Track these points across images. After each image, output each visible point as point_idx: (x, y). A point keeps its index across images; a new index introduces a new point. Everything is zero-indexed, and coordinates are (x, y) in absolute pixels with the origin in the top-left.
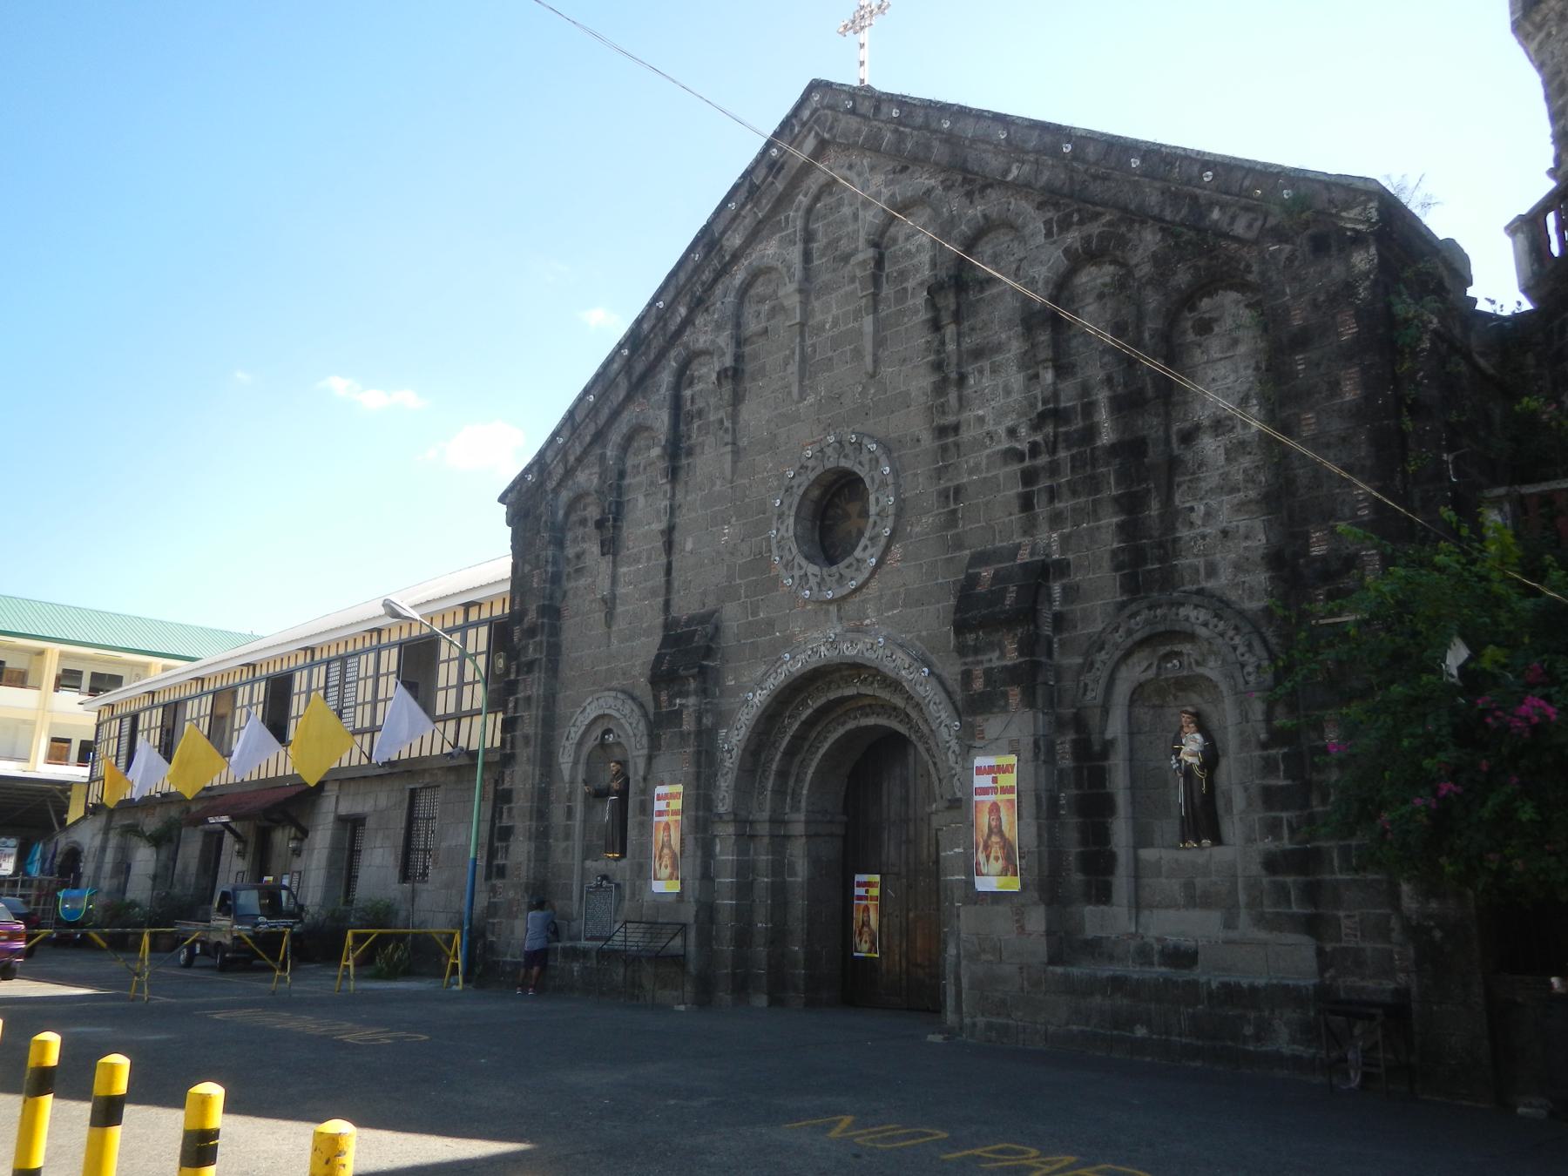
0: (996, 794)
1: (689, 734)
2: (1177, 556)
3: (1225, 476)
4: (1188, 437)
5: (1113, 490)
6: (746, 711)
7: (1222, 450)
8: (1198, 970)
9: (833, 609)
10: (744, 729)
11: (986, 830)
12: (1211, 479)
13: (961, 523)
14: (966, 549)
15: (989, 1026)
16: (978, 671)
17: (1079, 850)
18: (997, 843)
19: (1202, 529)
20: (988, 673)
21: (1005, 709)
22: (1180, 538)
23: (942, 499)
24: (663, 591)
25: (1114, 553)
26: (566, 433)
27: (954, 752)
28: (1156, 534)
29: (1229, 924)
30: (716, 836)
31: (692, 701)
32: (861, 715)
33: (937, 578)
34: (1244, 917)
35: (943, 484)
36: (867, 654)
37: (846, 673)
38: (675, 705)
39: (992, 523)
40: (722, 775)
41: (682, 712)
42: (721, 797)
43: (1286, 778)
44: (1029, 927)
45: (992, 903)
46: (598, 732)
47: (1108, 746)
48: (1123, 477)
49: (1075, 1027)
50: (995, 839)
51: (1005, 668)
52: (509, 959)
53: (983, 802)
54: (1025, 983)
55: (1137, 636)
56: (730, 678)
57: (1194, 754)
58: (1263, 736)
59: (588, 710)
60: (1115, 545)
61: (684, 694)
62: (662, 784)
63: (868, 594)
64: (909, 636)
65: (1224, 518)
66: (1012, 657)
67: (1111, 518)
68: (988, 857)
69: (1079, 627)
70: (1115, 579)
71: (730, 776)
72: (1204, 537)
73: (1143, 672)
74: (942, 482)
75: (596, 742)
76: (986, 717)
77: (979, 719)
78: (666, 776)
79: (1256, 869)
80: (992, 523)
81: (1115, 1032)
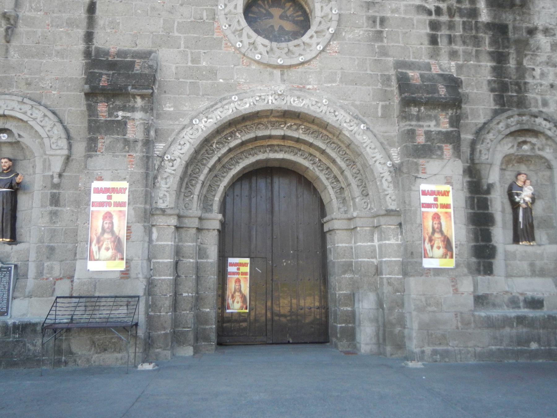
0: (437, 208)
1: (136, 141)
2: (526, 91)
3: (549, 57)
4: (532, 32)
5: (487, 47)
6: (191, 132)
7: (549, 44)
8: (545, 309)
9: (277, 72)
11: (430, 230)
12: (542, 57)
13: (385, 40)
14: (389, 56)
15: (435, 352)
16: (420, 132)
17: (473, 244)
18: (438, 238)
19: (539, 81)
20: (428, 134)
21: (441, 157)
22: (528, 83)
23: (371, 22)
24: (85, 23)
25: (489, 82)
27: (386, 180)
28: (514, 77)
30: (153, 226)
31: (139, 115)
33: (366, 70)
35: (371, 13)
36: (312, 108)
37: (274, 119)
39: (408, 46)
40: (162, 179)
41: (126, 124)
42: (161, 195)
44: (461, 289)
45: (434, 275)
47: (490, 187)
48: (493, 42)
49: (493, 347)
50: (437, 235)
51: (440, 132)
53: (427, 212)
54: (459, 323)
55: (513, 129)
56: (168, 105)
57: (527, 196)
60: (489, 78)
61: (133, 109)
62: (100, 179)
63: (309, 68)
64: (346, 102)
66: (445, 126)
67: (487, 62)
68: (432, 247)
69: (470, 117)
70: (490, 96)
72: (541, 85)
73: (509, 149)
74: (370, 11)
76: (427, 160)
77: (421, 161)
81: (519, 348)
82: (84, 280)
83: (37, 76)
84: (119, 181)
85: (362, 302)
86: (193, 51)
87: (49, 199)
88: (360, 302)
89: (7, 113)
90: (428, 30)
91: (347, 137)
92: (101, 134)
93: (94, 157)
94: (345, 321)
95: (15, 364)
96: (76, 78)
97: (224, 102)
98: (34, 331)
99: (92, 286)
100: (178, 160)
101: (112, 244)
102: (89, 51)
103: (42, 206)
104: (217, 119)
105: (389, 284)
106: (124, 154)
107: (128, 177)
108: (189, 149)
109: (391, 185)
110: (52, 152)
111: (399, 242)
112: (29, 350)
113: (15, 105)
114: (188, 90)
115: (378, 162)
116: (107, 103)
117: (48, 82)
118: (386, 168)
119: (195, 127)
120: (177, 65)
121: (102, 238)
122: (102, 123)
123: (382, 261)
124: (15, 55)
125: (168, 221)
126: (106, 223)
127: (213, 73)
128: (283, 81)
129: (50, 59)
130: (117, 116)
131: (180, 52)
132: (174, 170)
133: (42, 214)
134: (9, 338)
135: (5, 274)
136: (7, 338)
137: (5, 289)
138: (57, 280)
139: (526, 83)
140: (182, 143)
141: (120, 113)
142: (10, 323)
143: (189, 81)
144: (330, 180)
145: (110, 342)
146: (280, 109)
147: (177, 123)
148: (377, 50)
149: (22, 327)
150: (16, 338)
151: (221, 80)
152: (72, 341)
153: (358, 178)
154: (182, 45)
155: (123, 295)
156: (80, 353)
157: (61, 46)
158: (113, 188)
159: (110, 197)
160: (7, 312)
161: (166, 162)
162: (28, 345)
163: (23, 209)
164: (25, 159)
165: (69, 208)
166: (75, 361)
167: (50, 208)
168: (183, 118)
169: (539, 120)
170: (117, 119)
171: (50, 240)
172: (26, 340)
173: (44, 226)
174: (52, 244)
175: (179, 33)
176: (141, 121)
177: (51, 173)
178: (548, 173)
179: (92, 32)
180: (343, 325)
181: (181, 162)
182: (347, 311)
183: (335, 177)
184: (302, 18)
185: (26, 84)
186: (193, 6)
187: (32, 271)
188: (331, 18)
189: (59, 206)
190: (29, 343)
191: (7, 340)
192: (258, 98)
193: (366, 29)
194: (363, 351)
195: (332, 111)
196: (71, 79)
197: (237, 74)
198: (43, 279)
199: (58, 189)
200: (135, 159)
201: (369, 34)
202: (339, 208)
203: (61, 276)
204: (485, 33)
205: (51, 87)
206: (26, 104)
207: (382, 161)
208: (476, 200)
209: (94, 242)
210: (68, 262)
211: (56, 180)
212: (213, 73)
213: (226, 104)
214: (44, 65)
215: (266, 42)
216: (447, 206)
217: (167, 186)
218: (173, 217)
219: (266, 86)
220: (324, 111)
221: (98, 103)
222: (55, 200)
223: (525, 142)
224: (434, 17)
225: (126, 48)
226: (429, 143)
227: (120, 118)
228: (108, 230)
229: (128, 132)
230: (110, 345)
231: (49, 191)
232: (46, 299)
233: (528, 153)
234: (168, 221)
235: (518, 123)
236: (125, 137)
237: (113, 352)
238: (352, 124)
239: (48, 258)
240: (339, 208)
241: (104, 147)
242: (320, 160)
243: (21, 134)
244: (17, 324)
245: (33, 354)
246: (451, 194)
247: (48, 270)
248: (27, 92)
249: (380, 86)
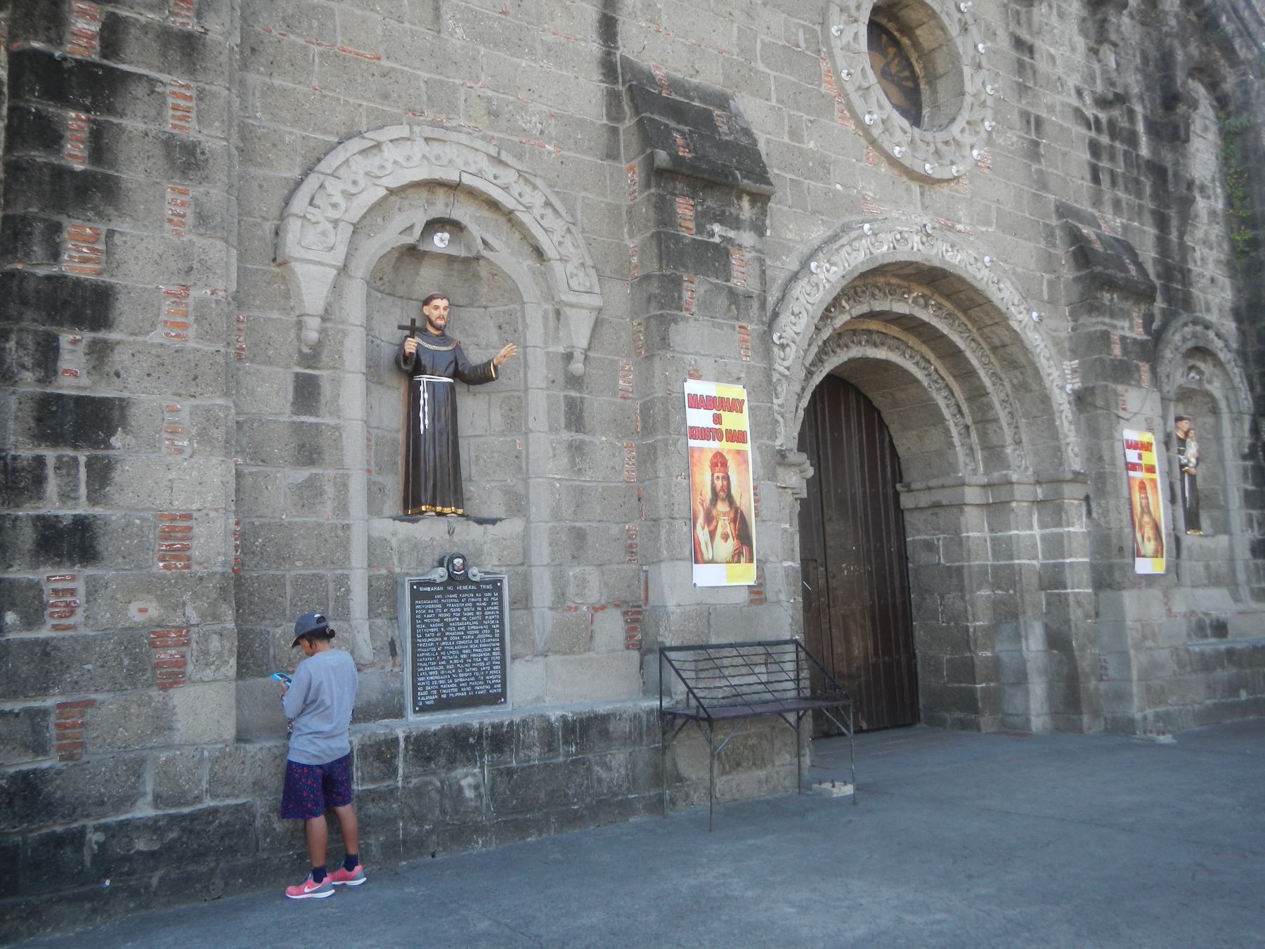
9: (915, 188)
10: (804, 319)
12: (1199, 234)
14: (1050, 192)
16: (1115, 336)
21: (1139, 386)
29: (1237, 599)
32: (867, 341)
34: (1244, 592)
37: (893, 281)
38: (713, 235)
39: (1068, 178)
41: (727, 254)
43: (1253, 485)
46: (419, 219)
48: (1155, 196)
52: (144, 810)
58: (1246, 450)
59: (390, 153)
62: (696, 375)
63: (957, 191)
74: (1024, 102)
75: (410, 240)
77: (1120, 388)
78: (706, 364)
79: (1248, 555)
80: (1068, 178)
82: (688, 608)
83: (511, 98)
84: (728, 382)
85: (1027, 639)
86: (792, 113)
87: (562, 412)
88: (1023, 641)
89: (467, 180)
90: (1087, 156)
91: (1015, 331)
92: (687, 271)
93: (681, 323)
94: (987, 679)
95: (573, 819)
96: (592, 123)
97: (853, 234)
98: (605, 734)
99: (704, 621)
101: (732, 524)
102: (611, 62)
103: (553, 430)
104: (844, 267)
105: (1079, 603)
106: (731, 322)
107: (743, 375)
108: (808, 325)
109: (1073, 427)
110: (572, 298)
111: (1084, 530)
112: (600, 781)
113: (484, 163)
114: (789, 197)
115: (1055, 384)
116: (693, 199)
117: (535, 119)
118: (1064, 396)
119: (814, 278)
120: (768, 136)
121: (714, 512)
122: (686, 244)
123: (1063, 564)
124: (457, 30)
125: (787, 477)
126: (718, 478)
127: (823, 167)
128: (925, 207)
129: (535, 61)
130: (713, 235)
131: (772, 108)
132: (788, 368)
133: (554, 449)
134: (558, 756)
135: (489, 597)
136: (553, 757)
137: (494, 637)
138: (596, 610)
139: (1189, 271)
140: (796, 310)
141: (717, 228)
142: (553, 719)
143: (789, 176)
144: (952, 409)
145: (745, 746)
146: (928, 264)
147: (778, 264)
148: (1035, 177)
149: (581, 728)
150: (572, 755)
151: (838, 187)
152: (678, 750)
153: (1007, 410)
154: (774, 96)
155: (758, 638)
156: (694, 777)
157: (554, 34)
158: (722, 399)
159: (717, 419)
160: (503, 694)
161: (776, 349)
162: (597, 768)
163: (470, 432)
164: (471, 305)
165: (604, 439)
166: (687, 795)
167: (567, 436)
168: (787, 256)
169: (1211, 334)
170: (712, 240)
171: (575, 513)
172: (590, 756)
173: (560, 479)
174: (578, 524)
175: (768, 65)
176: (754, 254)
177: (561, 350)
178: (1210, 420)
179: (612, 18)
180: (984, 685)
181: (797, 351)
182: (987, 658)
183: (958, 406)
184: (910, 84)
185: (489, 113)
186: (783, 12)
187: (543, 594)
188: (984, 101)
189: (584, 433)
190: (597, 764)
191: (553, 761)
192: (898, 236)
193: (1020, 133)
194: (1034, 729)
195: (995, 280)
196: (581, 123)
197: (862, 180)
198: (570, 608)
199: (580, 389)
200: (749, 337)
201: (1022, 143)
202: (966, 465)
203: (603, 602)
204: (1147, 178)
205: (542, 132)
206: (506, 165)
207: (1060, 383)
209: (701, 520)
210: (614, 567)
211: (577, 367)
212: (823, 167)
213: (855, 239)
214: (523, 72)
215: (905, 123)
216: (1151, 469)
217: (779, 401)
218: (793, 469)
219: (903, 214)
220: (986, 279)
221: (675, 195)
222: (575, 417)
223: (1191, 368)
224: (1093, 134)
225: (679, 76)
226: (1125, 358)
227: (717, 240)
228: (722, 494)
229: (735, 274)
230: (746, 752)
231: (562, 394)
232: (578, 657)
234: (787, 477)
235: (1195, 335)
236: (728, 284)
237: (750, 768)
238: (1022, 308)
239: (574, 557)
240: (966, 465)
241: (694, 301)
242: (936, 370)
243: (490, 240)
244: (570, 719)
245: (609, 788)
246: (1154, 448)
247: (578, 586)
248: (491, 133)
249: (1042, 245)
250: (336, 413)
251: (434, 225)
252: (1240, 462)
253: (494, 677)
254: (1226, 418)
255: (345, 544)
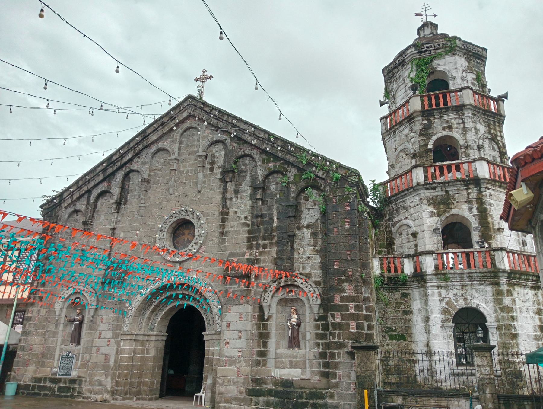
9: (178, 265)
13: (226, 243)
14: (227, 251)
19: (302, 256)
26: (75, 188)
46: (73, 297)
58: (317, 318)
65: (308, 254)
66: (243, 288)
71: (130, 318)
72: (303, 258)
100: (134, 309)
208: (261, 325)
211: (91, 319)
233: (294, 297)
250: (59, 330)
251: (76, 298)
252: (315, 323)
253: (70, 372)
254: (307, 307)
255: (56, 349)
